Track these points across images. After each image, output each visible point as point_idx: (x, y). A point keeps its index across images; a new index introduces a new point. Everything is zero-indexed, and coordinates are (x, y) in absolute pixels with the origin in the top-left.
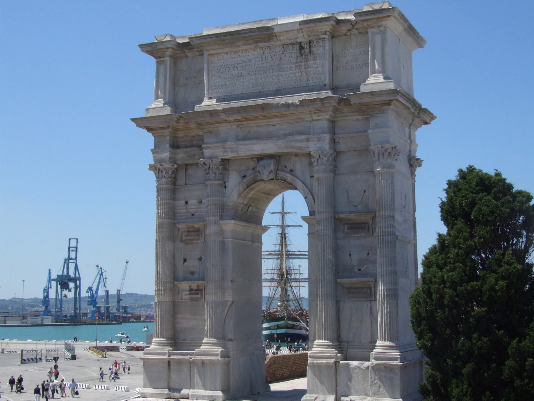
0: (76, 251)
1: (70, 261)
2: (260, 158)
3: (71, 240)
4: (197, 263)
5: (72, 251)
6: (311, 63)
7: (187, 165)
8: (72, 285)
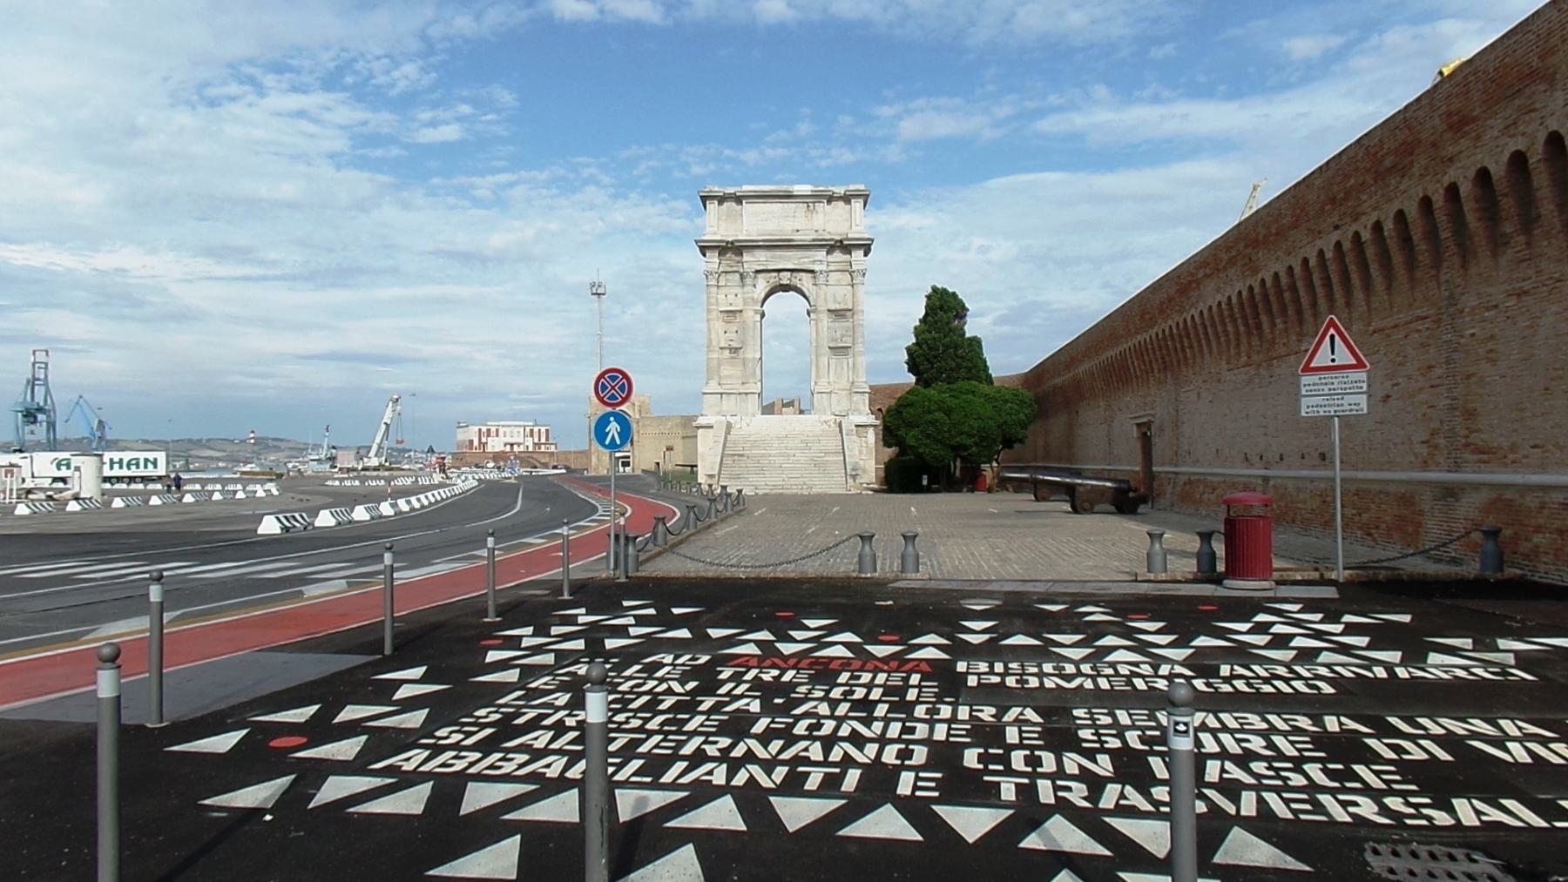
0: (46, 368)
1: (37, 382)
2: (779, 271)
3: (37, 353)
4: (735, 335)
5: (39, 368)
6: (814, 214)
7: (726, 272)
8: (41, 417)
